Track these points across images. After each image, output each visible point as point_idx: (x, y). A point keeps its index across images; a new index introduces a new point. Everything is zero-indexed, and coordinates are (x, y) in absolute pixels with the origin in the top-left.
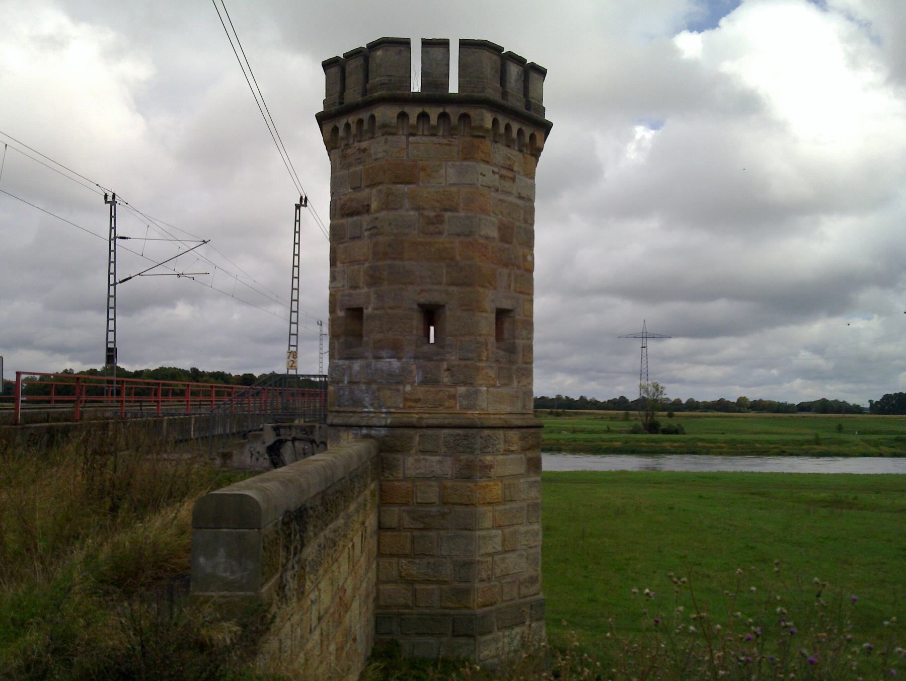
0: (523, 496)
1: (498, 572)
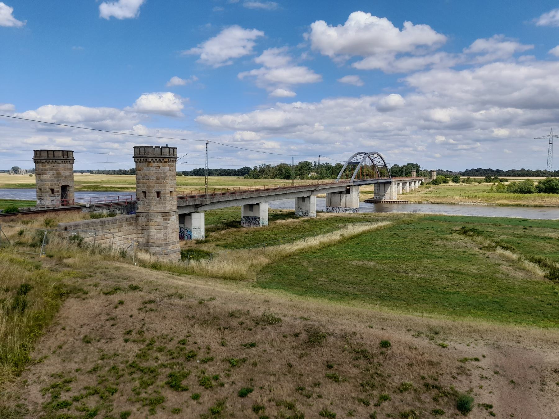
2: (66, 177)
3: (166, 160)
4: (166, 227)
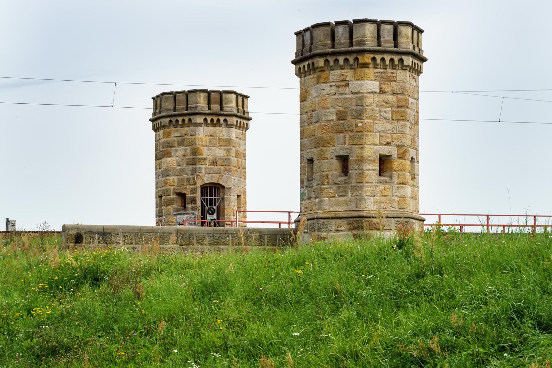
3: (367, 59)
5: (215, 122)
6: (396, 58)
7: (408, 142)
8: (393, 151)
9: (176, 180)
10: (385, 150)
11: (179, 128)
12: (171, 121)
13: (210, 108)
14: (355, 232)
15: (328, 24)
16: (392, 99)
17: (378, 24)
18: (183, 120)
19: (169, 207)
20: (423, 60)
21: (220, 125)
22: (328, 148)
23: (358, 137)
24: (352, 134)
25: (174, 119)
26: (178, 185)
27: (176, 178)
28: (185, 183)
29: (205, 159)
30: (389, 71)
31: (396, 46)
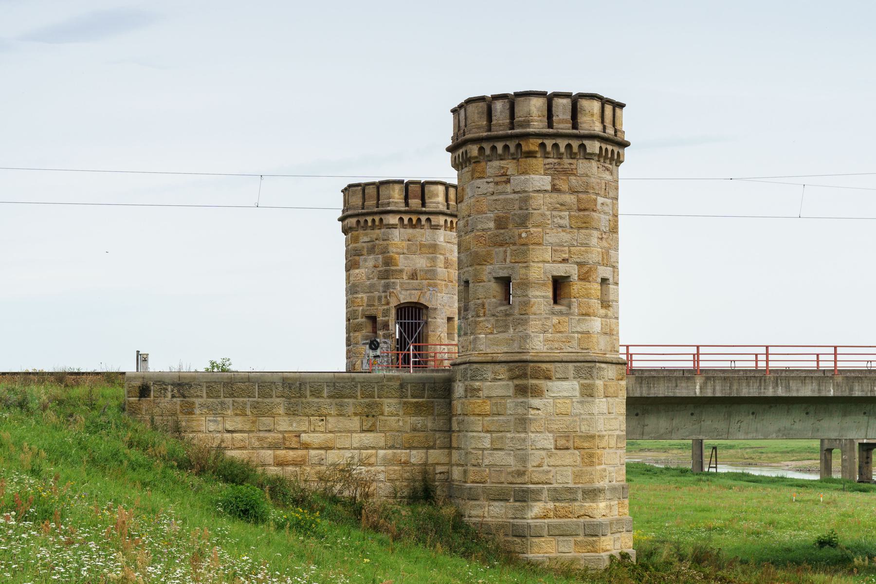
0: (509, 412)
1: (486, 462)
2: (414, 276)
3: (533, 145)
4: (523, 423)
5: (414, 222)
6: (575, 144)
7: (594, 256)
8: (572, 270)
9: (365, 299)
10: (560, 270)
11: (369, 231)
12: (358, 222)
13: (407, 204)
14: (517, 382)
15: (482, 99)
16: (570, 199)
17: (550, 99)
18: (374, 220)
19: (357, 334)
20: (624, 145)
21: (422, 227)
22: (484, 267)
23: (522, 251)
24: (515, 248)
25: (362, 220)
26: (368, 305)
27: (365, 296)
28: (376, 303)
29: (401, 271)
30: (566, 161)
31: (575, 126)
